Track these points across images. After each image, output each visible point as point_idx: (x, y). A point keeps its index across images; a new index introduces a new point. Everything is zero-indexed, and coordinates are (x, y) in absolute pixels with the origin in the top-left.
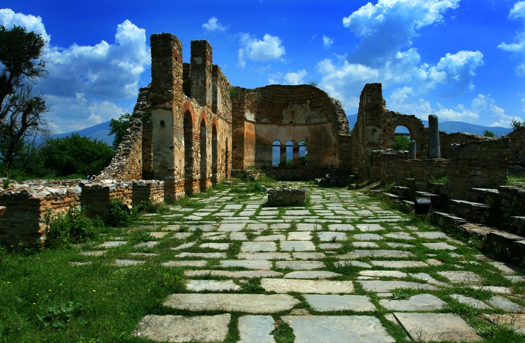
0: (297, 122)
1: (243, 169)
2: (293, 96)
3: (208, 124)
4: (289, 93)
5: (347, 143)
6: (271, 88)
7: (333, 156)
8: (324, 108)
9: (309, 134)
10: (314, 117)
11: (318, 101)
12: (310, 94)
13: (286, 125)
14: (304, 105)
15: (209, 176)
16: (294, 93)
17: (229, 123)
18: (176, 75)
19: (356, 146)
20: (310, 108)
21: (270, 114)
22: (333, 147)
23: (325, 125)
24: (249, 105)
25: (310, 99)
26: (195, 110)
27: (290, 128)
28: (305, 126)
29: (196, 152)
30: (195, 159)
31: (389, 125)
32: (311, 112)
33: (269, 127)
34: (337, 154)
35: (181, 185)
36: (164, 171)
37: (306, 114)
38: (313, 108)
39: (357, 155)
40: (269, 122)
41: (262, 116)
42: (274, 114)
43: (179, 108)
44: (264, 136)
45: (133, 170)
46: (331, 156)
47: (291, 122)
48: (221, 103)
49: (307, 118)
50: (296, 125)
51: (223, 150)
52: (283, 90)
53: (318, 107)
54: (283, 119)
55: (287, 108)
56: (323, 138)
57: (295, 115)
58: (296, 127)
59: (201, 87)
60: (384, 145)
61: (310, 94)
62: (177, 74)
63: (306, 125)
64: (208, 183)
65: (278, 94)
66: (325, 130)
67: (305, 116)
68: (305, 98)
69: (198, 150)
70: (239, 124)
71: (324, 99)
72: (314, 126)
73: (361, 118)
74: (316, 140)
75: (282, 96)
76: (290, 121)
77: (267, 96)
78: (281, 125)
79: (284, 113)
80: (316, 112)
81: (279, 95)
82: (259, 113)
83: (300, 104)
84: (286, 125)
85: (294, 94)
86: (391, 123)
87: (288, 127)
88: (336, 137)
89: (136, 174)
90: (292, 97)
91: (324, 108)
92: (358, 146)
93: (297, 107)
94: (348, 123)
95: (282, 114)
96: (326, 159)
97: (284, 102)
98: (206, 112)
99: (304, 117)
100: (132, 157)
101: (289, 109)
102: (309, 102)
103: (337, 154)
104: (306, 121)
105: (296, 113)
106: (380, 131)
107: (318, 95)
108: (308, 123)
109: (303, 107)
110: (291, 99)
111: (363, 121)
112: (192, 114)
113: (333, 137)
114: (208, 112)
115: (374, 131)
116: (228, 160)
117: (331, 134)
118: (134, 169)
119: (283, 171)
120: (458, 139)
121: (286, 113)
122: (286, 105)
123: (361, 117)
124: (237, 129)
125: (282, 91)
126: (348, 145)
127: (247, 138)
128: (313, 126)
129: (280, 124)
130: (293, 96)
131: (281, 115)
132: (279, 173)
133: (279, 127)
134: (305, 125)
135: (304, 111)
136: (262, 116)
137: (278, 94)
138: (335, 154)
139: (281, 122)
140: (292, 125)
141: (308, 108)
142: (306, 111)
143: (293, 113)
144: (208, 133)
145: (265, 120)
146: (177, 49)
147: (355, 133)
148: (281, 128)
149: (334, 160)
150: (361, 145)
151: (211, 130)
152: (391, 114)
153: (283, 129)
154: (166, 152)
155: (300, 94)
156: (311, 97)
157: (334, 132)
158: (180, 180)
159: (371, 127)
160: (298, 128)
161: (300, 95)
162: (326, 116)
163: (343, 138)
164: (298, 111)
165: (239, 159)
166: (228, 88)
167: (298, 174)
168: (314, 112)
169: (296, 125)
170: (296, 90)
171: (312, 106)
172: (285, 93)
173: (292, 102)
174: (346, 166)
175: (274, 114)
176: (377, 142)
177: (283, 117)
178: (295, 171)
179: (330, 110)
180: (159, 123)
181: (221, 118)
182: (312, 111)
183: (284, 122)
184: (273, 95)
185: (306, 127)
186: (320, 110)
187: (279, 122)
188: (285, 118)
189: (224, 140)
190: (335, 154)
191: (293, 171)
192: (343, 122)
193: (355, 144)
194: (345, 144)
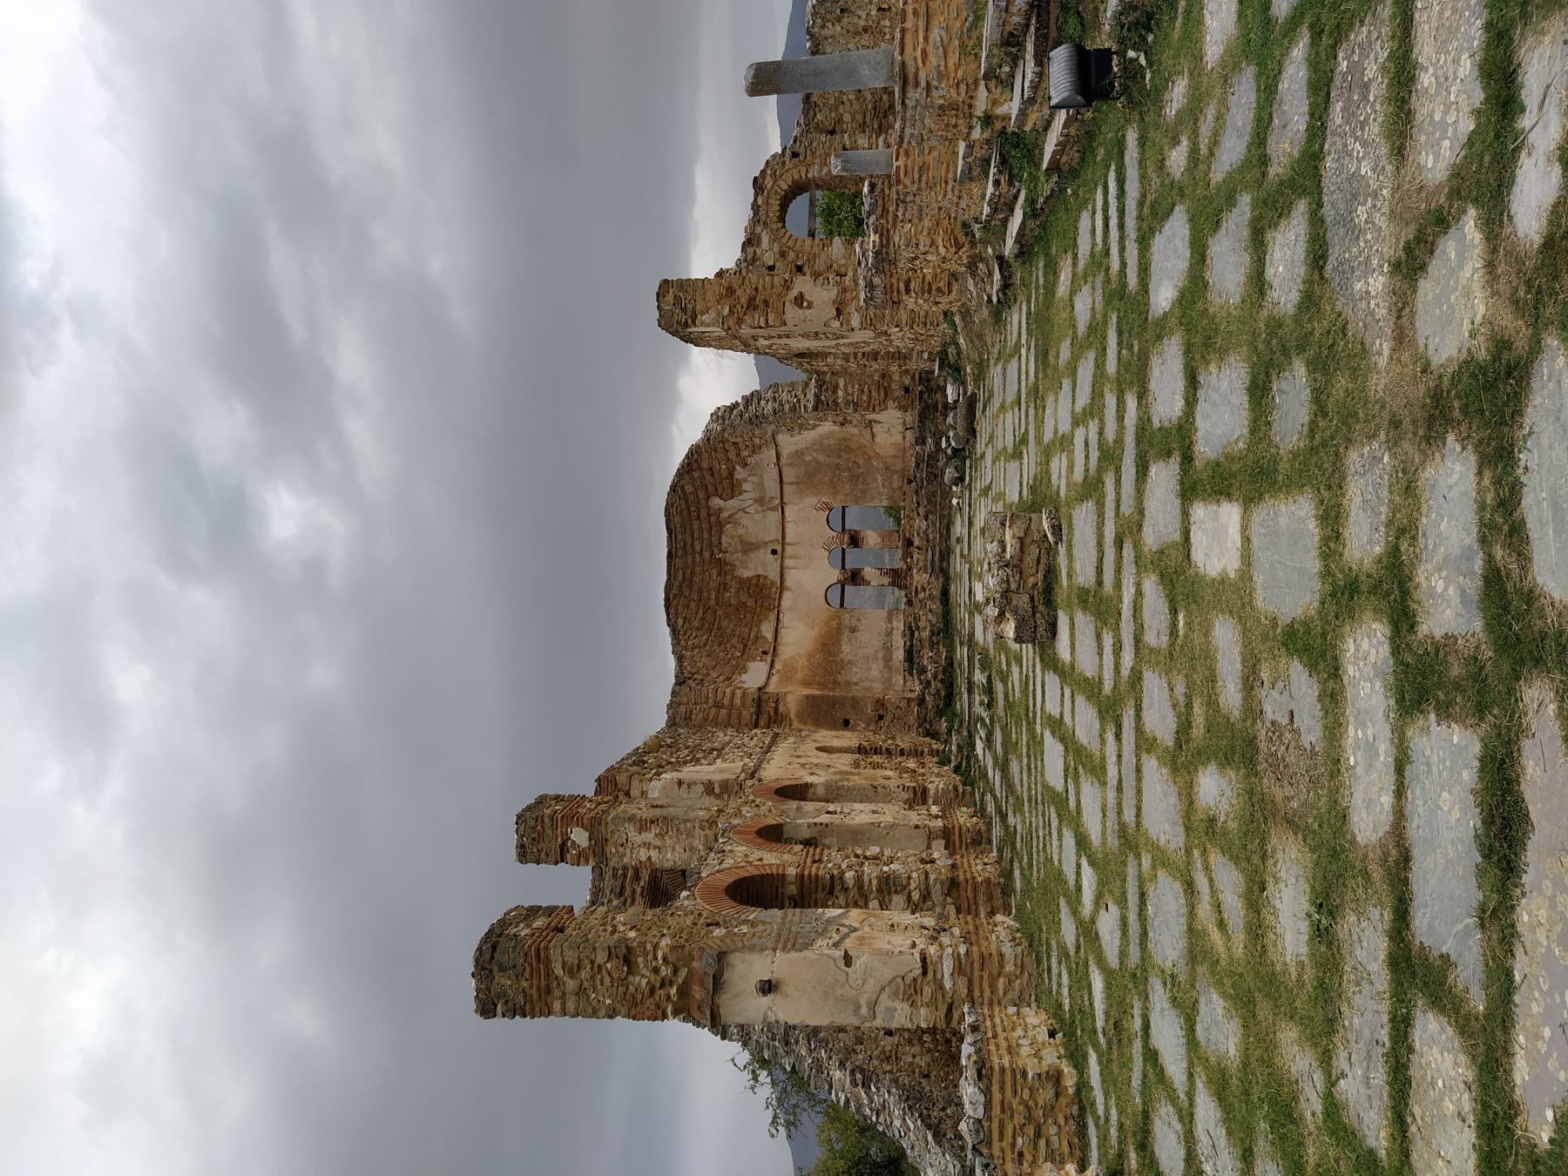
0: (775, 533)
1: (913, 699)
2: (698, 548)
3: (771, 812)
5: (836, 387)
6: (672, 610)
7: (877, 428)
8: (732, 455)
10: (760, 486)
11: (713, 475)
14: (725, 514)
15: (937, 817)
17: (774, 741)
18: (613, 933)
19: (846, 358)
20: (733, 497)
22: (850, 429)
23: (785, 453)
24: (721, 678)
25: (708, 498)
26: (729, 862)
27: (791, 558)
28: (786, 514)
29: (862, 864)
30: (886, 869)
31: (783, 255)
32: (746, 496)
33: (786, 619)
34: (870, 416)
35: (971, 928)
36: (927, 990)
38: (732, 488)
39: (875, 356)
40: (773, 616)
41: (757, 638)
42: (750, 603)
43: (717, 924)
44: (814, 633)
45: (918, 1059)
46: (873, 436)
47: (774, 552)
48: (712, 768)
49: (762, 505)
50: (783, 539)
51: (856, 765)
52: (680, 577)
53: (731, 475)
56: (821, 458)
57: (753, 540)
58: (788, 540)
59: (661, 836)
60: (843, 270)
61: (691, 498)
62: (610, 929)
63: (782, 508)
64: (962, 820)
66: (798, 454)
69: (857, 856)
70: (776, 709)
71: (705, 456)
72: (785, 486)
73: (762, 342)
74: (826, 479)
77: (696, 624)
78: (782, 583)
79: (746, 574)
80: (746, 481)
81: (695, 588)
83: (720, 526)
85: (692, 545)
86: (776, 248)
87: (788, 562)
88: (820, 420)
89: (929, 1051)
90: (702, 550)
91: (732, 455)
92: (846, 350)
94: (776, 385)
95: (750, 580)
96: (882, 452)
97: (714, 572)
98: (736, 822)
99: (758, 516)
100: (876, 1063)
101: (736, 558)
102: (716, 502)
103: (870, 416)
104: (773, 509)
106: (803, 284)
107: (696, 474)
109: (731, 516)
110: (706, 554)
111: (771, 337)
112: (743, 874)
113: (820, 430)
114: (738, 814)
115: (800, 300)
116: (885, 746)
117: (809, 436)
118: (914, 1056)
119: (916, 577)
120: (826, 32)
122: (723, 567)
123: (758, 343)
124: (793, 716)
126: (842, 383)
127: (819, 684)
128: (787, 489)
129: (782, 588)
130: (698, 548)
131: (754, 582)
132: (924, 590)
133: (789, 589)
135: (741, 513)
136: (757, 638)
138: (870, 424)
139: (773, 583)
141: (733, 503)
142: (743, 510)
143: (748, 547)
144: (803, 817)
145: (767, 630)
146: (528, 926)
147: (808, 363)
148: (789, 583)
149: (886, 426)
150: (842, 341)
151: (794, 804)
152: (750, 250)
153: (792, 577)
154: (865, 981)
155: (691, 525)
156: (701, 494)
157: (802, 427)
158: (956, 931)
159: (792, 313)
161: (696, 524)
162: (755, 450)
163: (823, 398)
164: (741, 531)
165: (881, 712)
166: (669, 741)
167: (927, 535)
168: (745, 486)
173: (716, 551)
174: (907, 390)
175: (750, 603)
176: (835, 291)
177: (759, 576)
178: (917, 542)
179: (739, 440)
180: (766, 1001)
181: (758, 767)
182: (740, 494)
183: (774, 575)
184: (693, 605)
185: (788, 509)
186: (737, 467)
188: (760, 572)
189: (824, 758)
190: (870, 422)
191: (918, 548)
192: (775, 399)
193: (839, 362)
194: (840, 393)
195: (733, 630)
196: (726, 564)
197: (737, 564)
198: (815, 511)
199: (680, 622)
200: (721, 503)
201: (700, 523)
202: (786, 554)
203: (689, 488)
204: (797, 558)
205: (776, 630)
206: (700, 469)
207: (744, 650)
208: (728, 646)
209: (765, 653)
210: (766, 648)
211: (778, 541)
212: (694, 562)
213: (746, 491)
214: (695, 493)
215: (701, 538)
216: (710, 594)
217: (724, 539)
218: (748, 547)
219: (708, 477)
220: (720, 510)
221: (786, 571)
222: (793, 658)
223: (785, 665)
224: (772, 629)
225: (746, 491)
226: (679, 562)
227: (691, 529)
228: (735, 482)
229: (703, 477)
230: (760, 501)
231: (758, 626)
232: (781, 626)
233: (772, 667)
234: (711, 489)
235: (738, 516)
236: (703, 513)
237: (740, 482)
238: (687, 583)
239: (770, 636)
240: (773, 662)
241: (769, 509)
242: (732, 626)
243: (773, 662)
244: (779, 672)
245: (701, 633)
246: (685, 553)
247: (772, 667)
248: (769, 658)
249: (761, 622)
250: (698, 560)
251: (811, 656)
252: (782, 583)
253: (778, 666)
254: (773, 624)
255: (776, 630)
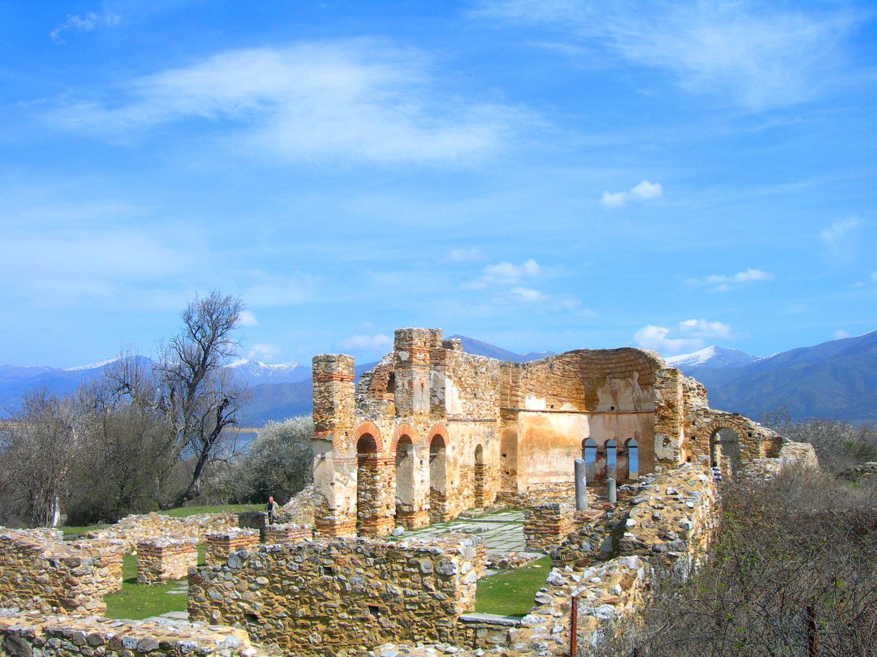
0: (622, 408)
2: (610, 366)
4: (605, 362)
9: (639, 430)
12: (636, 362)
13: (604, 413)
14: (630, 380)
16: (612, 361)
21: (575, 396)
25: (637, 371)
27: (609, 418)
28: (633, 415)
32: (641, 391)
37: (634, 395)
40: (575, 409)
47: (612, 408)
49: (637, 401)
50: (620, 414)
54: (598, 404)
55: (603, 385)
57: (618, 396)
58: (619, 416)
61: (636, 362)
63: (635, 413)
65: (586, 364)
67: (633, 398)
68: (630, 368)
75: (593, 366)
76: (610, 406)
78: (595, 413)
79: (599, 394)
81: (588, 366)
82: (556, 395)
83: (625, 378)
84: (604, 413)
85: (612, 363)
87: (607, 417)
90: (610, 368)
93: (619, 383)
95: (596, 395)
97: (598, 376)
99: (631, 399)
102: (636, 375)
104: (635, 407)
105: (618, 393)
108: (639, 409)
110: (608, 371)
121: (603, 392)
125: (593, 359)
130: (610, 366)
131: (595, 398)
134: (633, 413)
135: (631, 389)
137: (586, 364)
139: (595, 408)
140: (614, 414)
142: (634, 391)
143: (614, 394)
145: (567, 407)
156: (639, 367)
160: (625, 417)
161: (623, 364)
164: (622, 390)
168: (645, 392)
169: (619, 413)
170: (615, 356)
171: (643, 383)
172: (597, 362)
173: (610, 376)
177: (598, 400)
182: (641, 389)
183: (599, 408)
185: (635, 415)
187: (592, 409)
188: (601, 401)
195: (564, 388)
196: (604, 381)
197: (605, 388)
198: (634, 431)
199: (568, 359)
200: (636, 378)
201: (624, 367)
202: (611, 415)
203: (641, 361)
204: (609, 422)
205: (566, 412)
206: (651, 367)
207: (554, 395)
208: (555, 387)
209: (552, 407)
210: (555, 407)
211: (619, 411)
212: (603, 364)
213: (643, 392)
214: (639, 364)
215: (617, 367)
216: (587, 373)
217: (618, 380)
218: (614, 394)
219: (647, 372)
220: (633, 378)
221: (602, 415)
222: (549, 422)
223: (544, 419)
224: (567, 410)
225: (643, 392)
226: (601, 357)
227: (621, 362)
228: (647, 386)
229: (647, 368)
230: (639, 400)
231: (568, 401)
232: (569, 414)
233: (543, 412)
234: (643, 372)
235: (630, 387)
236: (630, 368)
237: (647, 389)
238: (590, 361)
239: (563, 408)
240: (546, 412)
241: (635, 405)
242: (567, 387)
243: (546, 412)
244: (539, 415)
245: (562, 370)
246: (606, 360)
247: (543, 412)
248: (549, 409)
249: (571, 402)
250: (604, 366)
251: (551, 432)
252: (595, 413)
253: (544, 415)
254: (571, 410)
255: (566, 412)
